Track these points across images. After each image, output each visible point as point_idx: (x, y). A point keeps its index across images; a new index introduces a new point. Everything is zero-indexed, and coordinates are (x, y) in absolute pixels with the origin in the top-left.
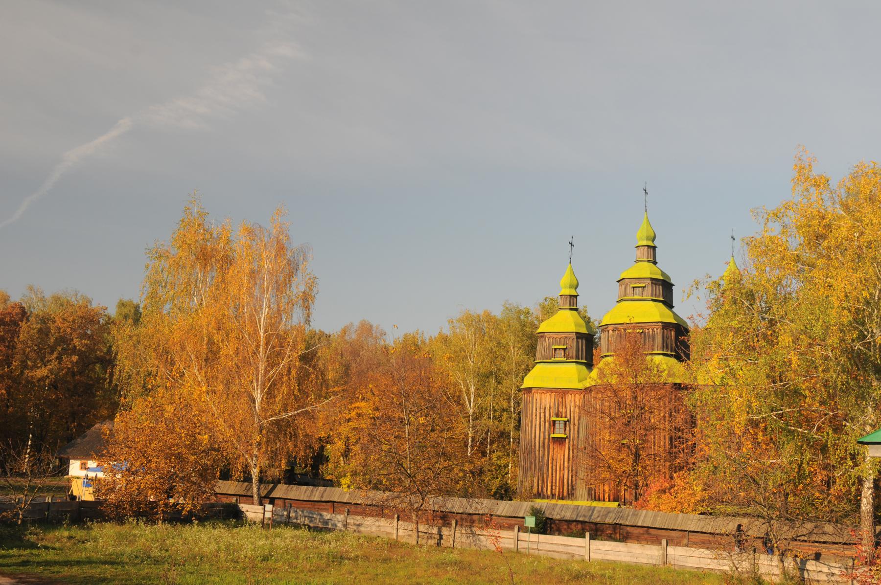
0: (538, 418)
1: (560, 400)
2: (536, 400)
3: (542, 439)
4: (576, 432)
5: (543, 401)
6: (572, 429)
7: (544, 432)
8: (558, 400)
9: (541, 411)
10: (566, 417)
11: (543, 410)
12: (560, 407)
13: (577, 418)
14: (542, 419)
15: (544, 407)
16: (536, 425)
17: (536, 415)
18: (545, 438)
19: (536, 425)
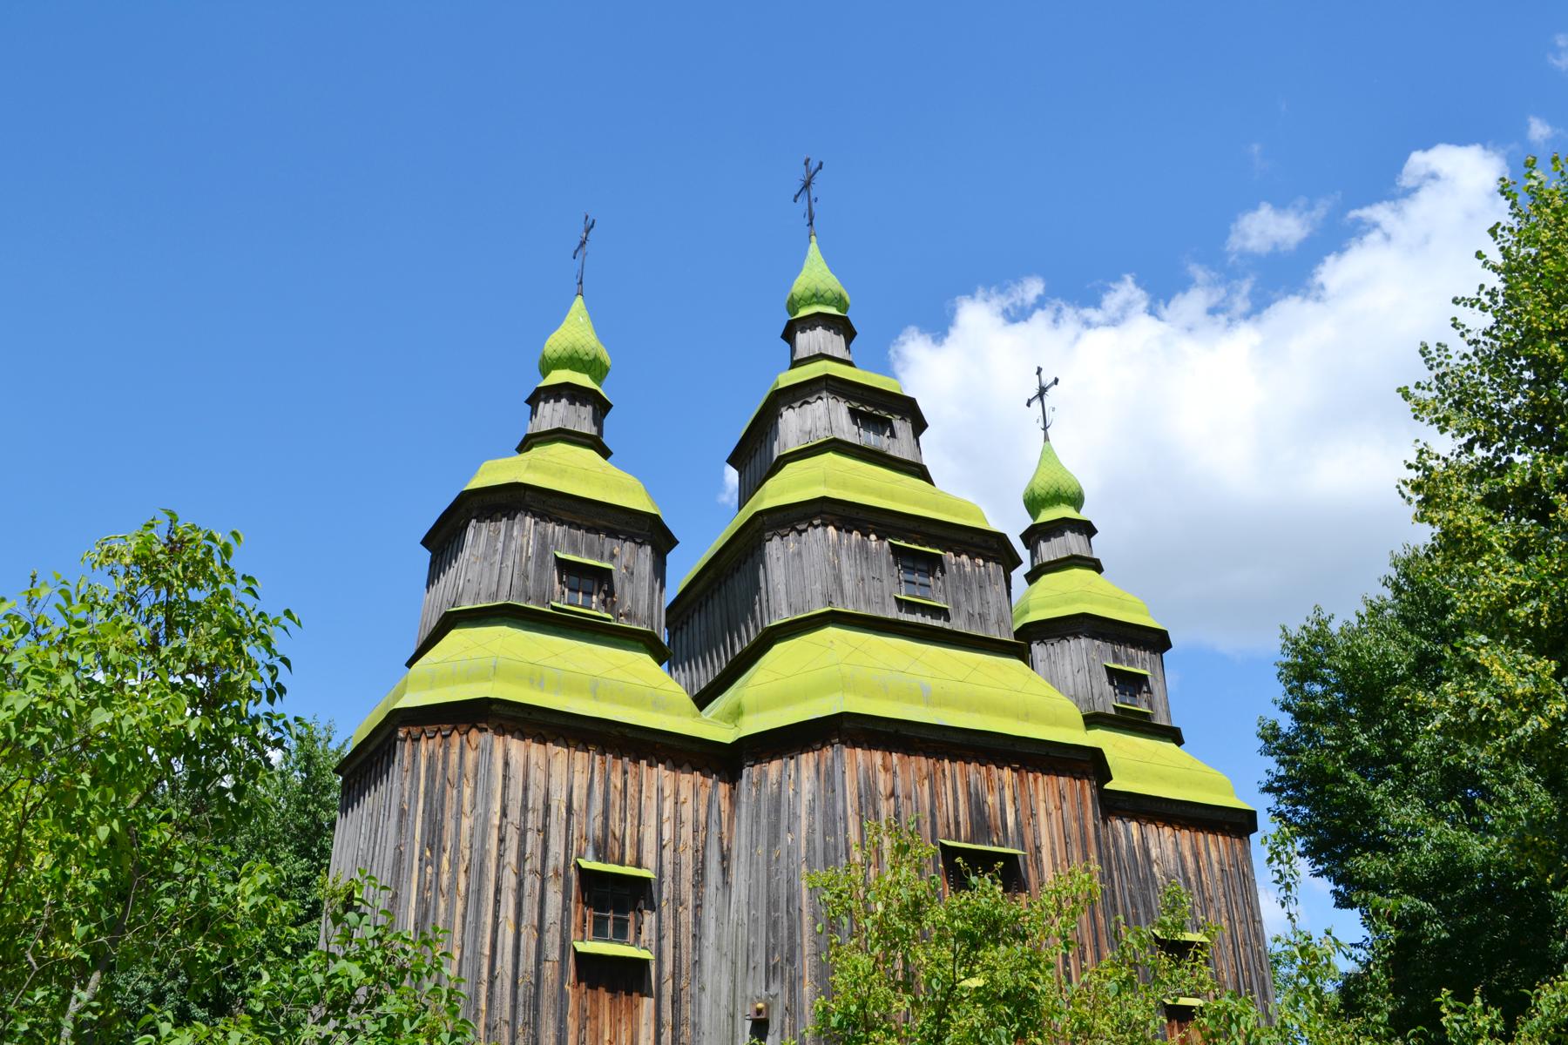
0: (511, 857)
1: (616, 780)
2: (506, 764)
3: (527, 963)
4: (687, 942)
5: (537, 776)
6: (668, 923)
7: (540, 929)
8: (607, 781)
9: (525, 821)
10: (639, 865)
11: (534, 820)
12: (615, 815)
13: (688, 873)
14: (533, 863)
15: (540, 806)
16: (498, 891)
17: (502, 840)
18: (540, 958)
19: (498, 891)
